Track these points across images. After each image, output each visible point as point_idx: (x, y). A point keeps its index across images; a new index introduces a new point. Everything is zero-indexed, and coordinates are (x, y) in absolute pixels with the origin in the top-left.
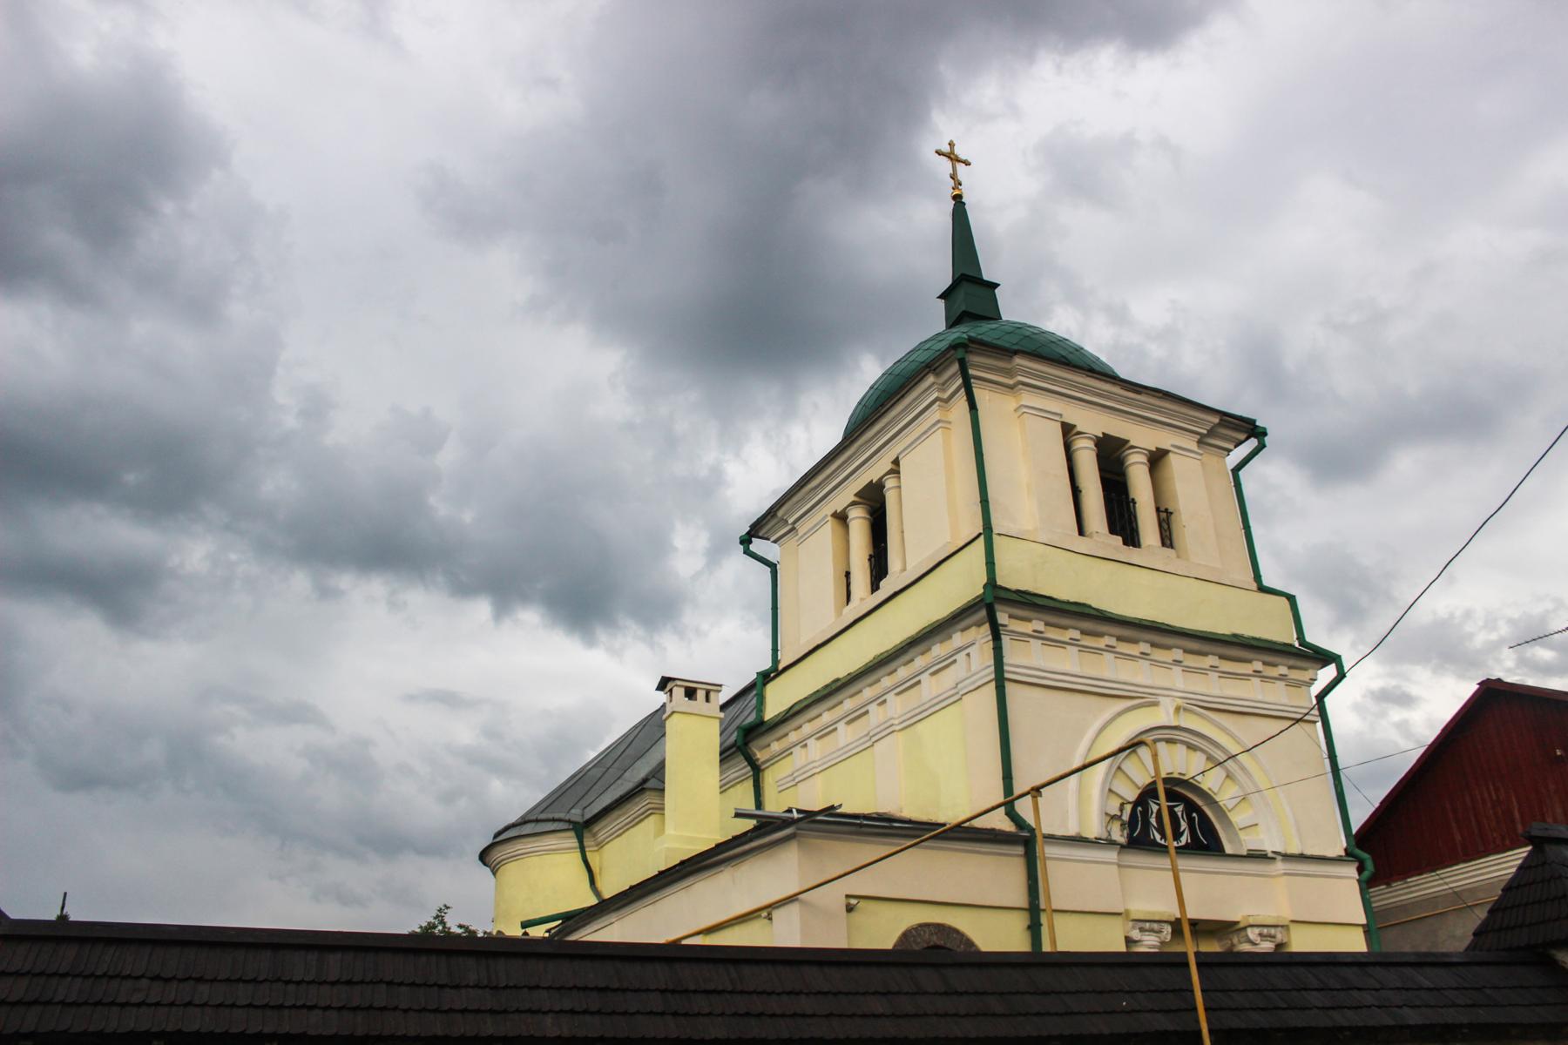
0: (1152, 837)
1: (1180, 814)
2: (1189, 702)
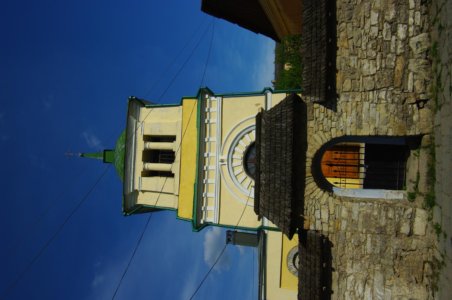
2: (219, 152)
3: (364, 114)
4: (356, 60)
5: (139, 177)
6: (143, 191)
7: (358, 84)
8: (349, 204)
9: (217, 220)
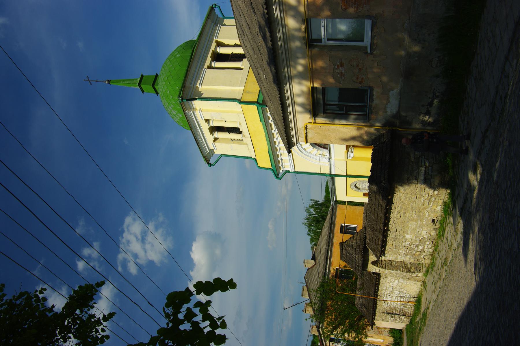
5: (213, 144)
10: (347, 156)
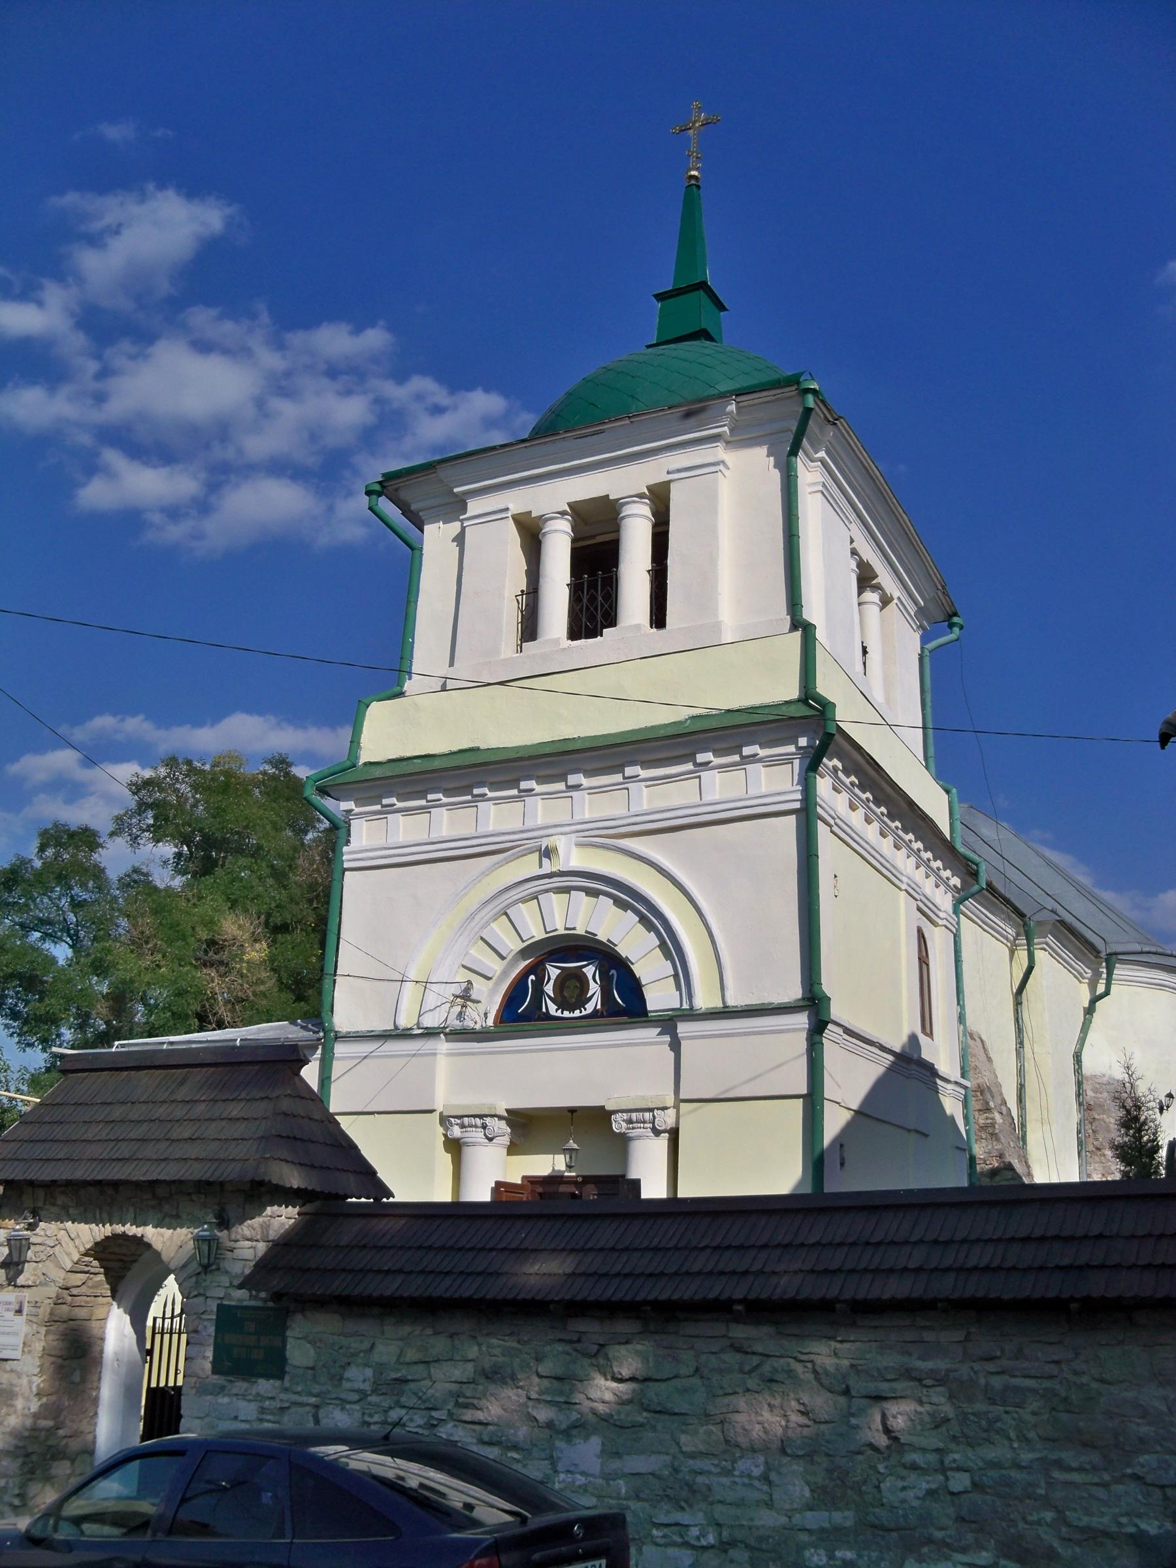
0: (544, 1010)
1: (590, 977)
3: (229, 1404)
4: (362, 1386)
5: (507, 509)
6: (460, 539)
7: (299, 1389)
8: (37, 1344)
9: (354, 860)
10: (474, 1116)
